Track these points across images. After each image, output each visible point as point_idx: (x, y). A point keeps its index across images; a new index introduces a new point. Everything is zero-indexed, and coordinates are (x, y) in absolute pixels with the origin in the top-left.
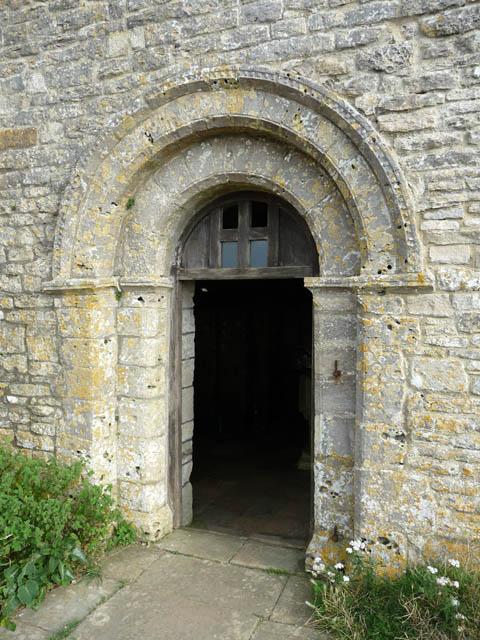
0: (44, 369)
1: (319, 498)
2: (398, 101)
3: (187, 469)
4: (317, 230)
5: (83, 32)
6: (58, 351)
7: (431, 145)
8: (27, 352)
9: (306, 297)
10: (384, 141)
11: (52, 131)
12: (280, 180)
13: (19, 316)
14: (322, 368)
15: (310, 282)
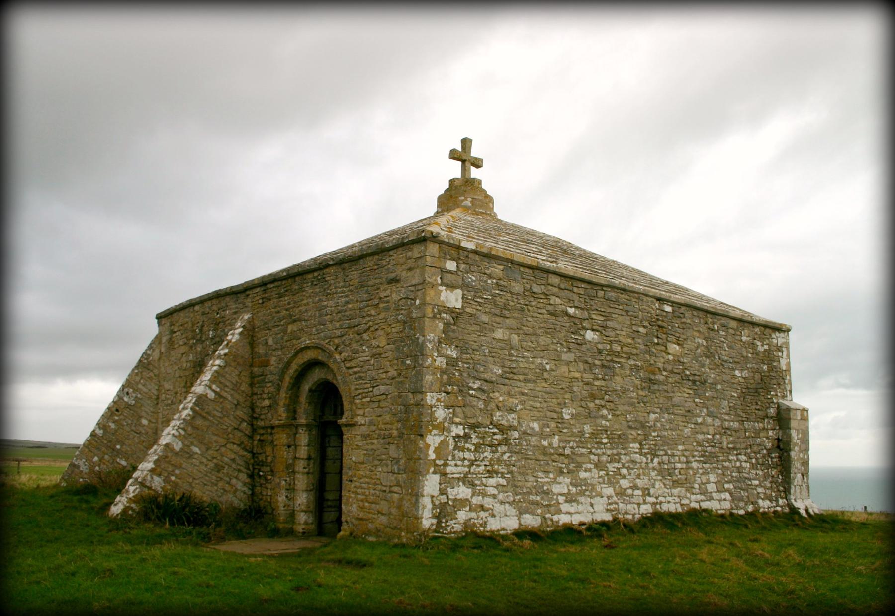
11: (273, 360)
15: (340, 421)
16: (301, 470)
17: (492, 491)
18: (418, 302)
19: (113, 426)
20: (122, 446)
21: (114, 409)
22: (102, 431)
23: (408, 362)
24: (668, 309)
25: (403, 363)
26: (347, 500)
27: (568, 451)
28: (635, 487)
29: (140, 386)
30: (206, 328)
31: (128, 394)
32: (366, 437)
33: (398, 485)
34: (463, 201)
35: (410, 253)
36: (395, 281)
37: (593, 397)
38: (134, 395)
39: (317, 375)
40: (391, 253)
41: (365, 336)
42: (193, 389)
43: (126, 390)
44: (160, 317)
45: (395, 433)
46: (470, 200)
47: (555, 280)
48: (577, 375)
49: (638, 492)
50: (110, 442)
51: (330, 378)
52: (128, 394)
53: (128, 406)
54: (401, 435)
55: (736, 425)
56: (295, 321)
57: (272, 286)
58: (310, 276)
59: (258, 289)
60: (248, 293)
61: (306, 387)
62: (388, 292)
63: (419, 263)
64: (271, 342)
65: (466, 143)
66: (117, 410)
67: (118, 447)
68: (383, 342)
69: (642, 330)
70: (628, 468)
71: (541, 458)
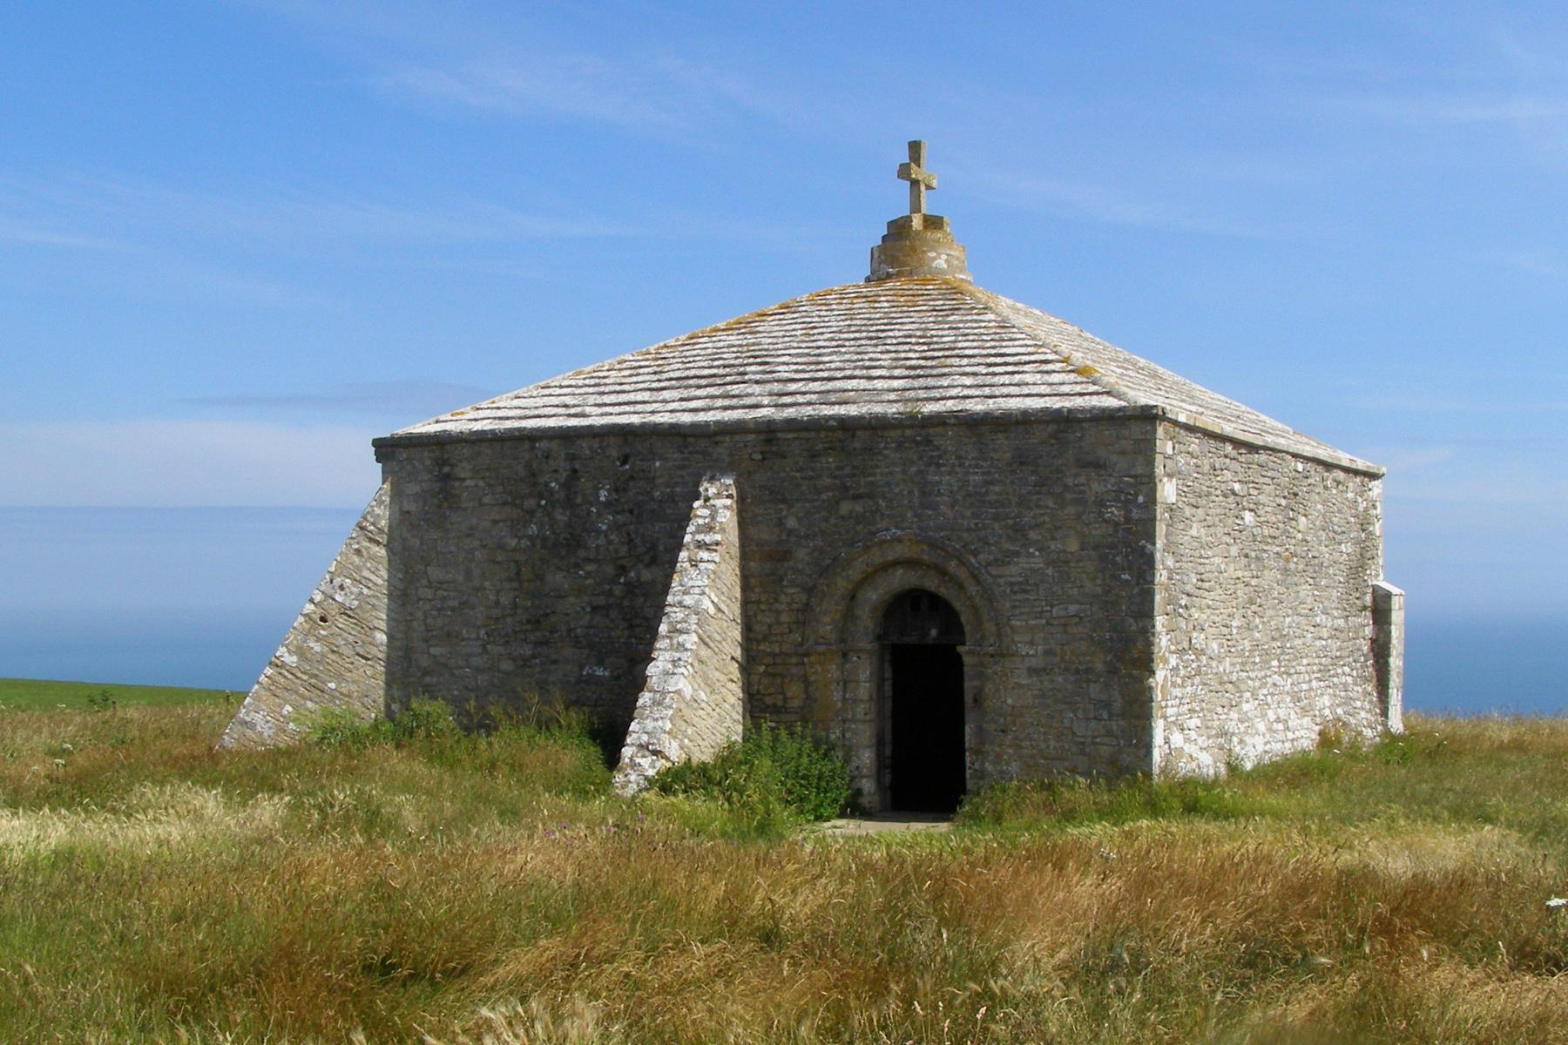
0: (796, 703)
1: (968, 772)
2: (996, 560)
3: (888, 779)
4: (963, 619)
5: (824, 497)
6: (806, 691)
7: (1012, 584)
8: (782, 693)
9: (959, 656)
10: (990, 580)
11: (801, 553)
12: (943, 592)
13: (779, 669)
14: (968, 698)
15: (960, 649)
16: (860, 716)
17: (1193, 735)
18: (1141, 499)
19: (317, 647)
20: (338, 684)
21: (317, 617)
22: (295, 658)
23: (1126, 577)
24: (1300, 467)
25: (1114, 577)
26: (998, 757)
27: (1234, 679)
28: (1278, 720)
29: (366, 573)
30: (584, 483)
31: (342, 588)
32: (1032, 671)
33: (1109, 733)
34: (934, 259)
35: (1126, 433)
36: (1098, 465)
37: (1252, 602)
38: (355, 590)
39: (900, 580)
40: (1086, 425)
41: (1033, 535)
42: (670, 599)
43: (337, 581)
44: (387, 449)
45: (1099, 667)
46: (944, 257)
47: (1229, 448)
48: (1240, 574)
49: (1281, 726)
50: (316, 676)
51: (931, 583)
52: (342, 588)
53: (346, 612)
54: (1112, 671)
55: (1341, 622)
56: (857, 497)
57: (790, 436)
58: (893, 433)
59: (751, 437)
60: (718, 438)
61: (874, 596)
62: (1082, 479)
63: (1146, 449)
64: (791, 523)
65: (915, 148)
66: (323, 619)
67: (332, 685)
68: (1073, 545)
69: (1283, 502)
70: (1273, 695)
71: (1219, 688)
